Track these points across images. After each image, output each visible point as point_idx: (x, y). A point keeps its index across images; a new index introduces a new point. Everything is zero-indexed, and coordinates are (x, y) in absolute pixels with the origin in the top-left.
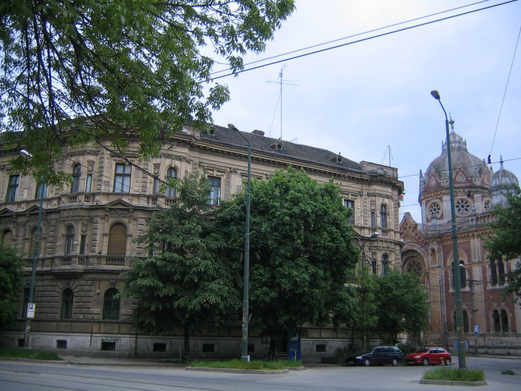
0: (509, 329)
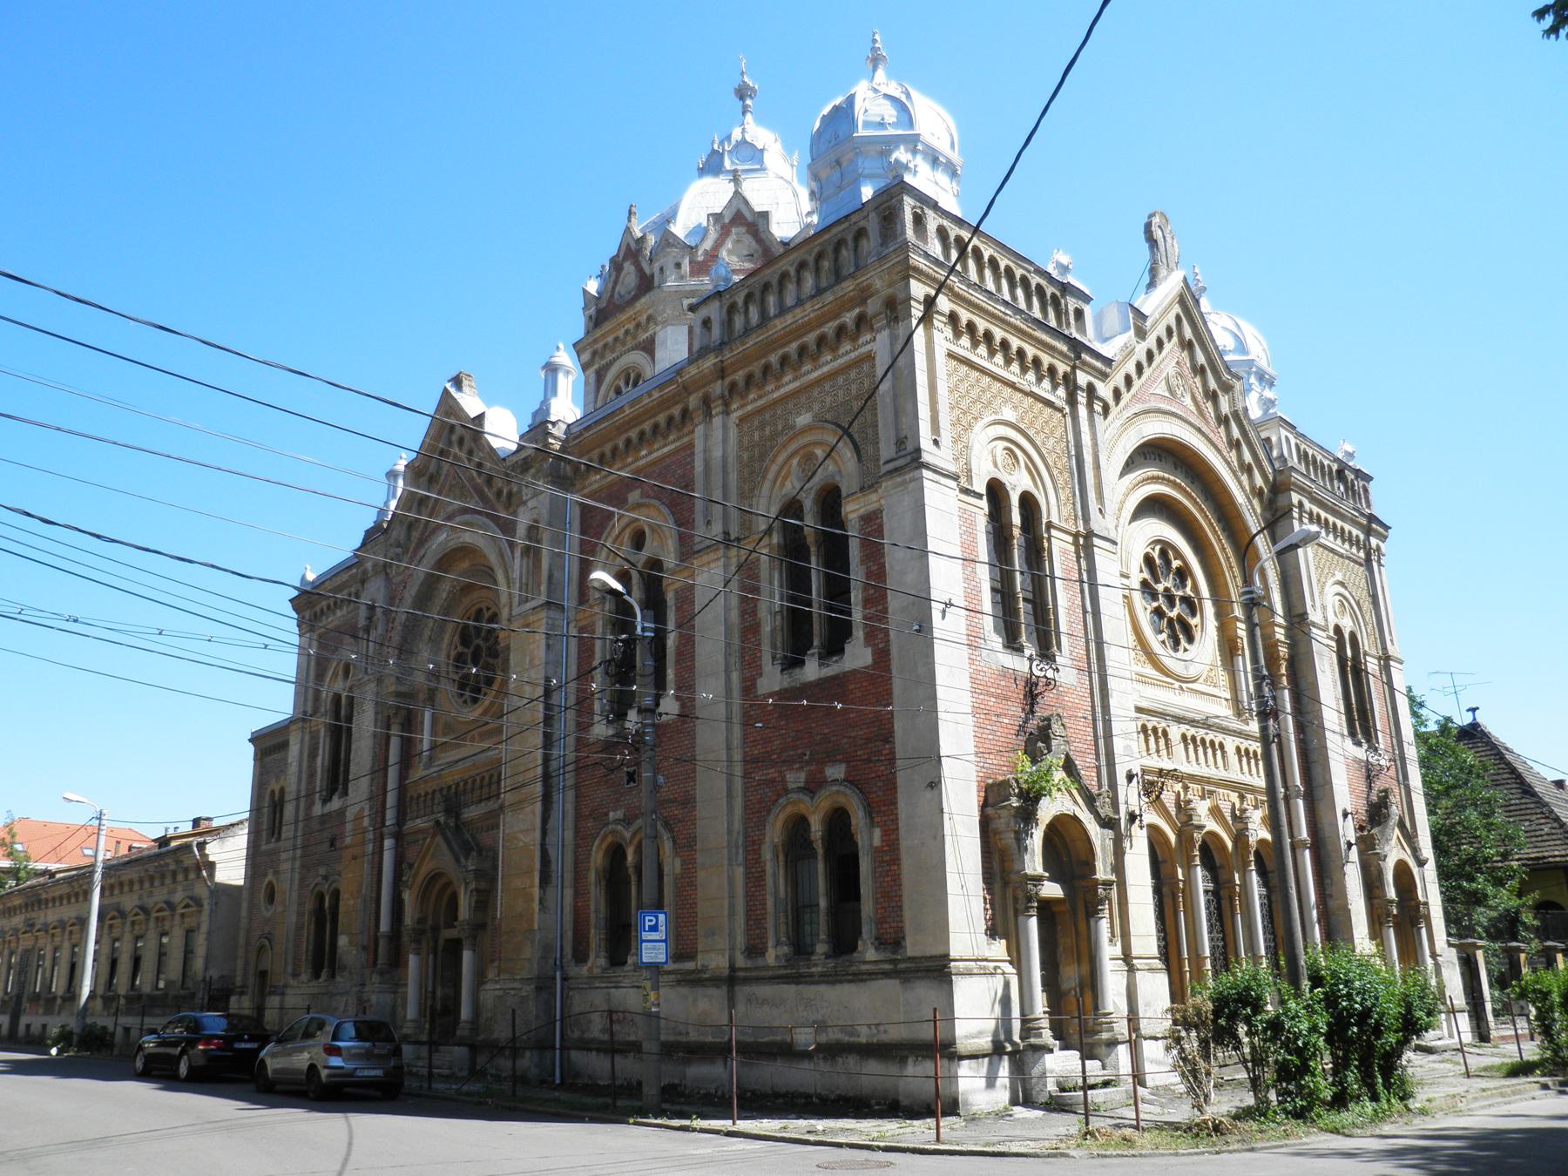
0: (867, 931)
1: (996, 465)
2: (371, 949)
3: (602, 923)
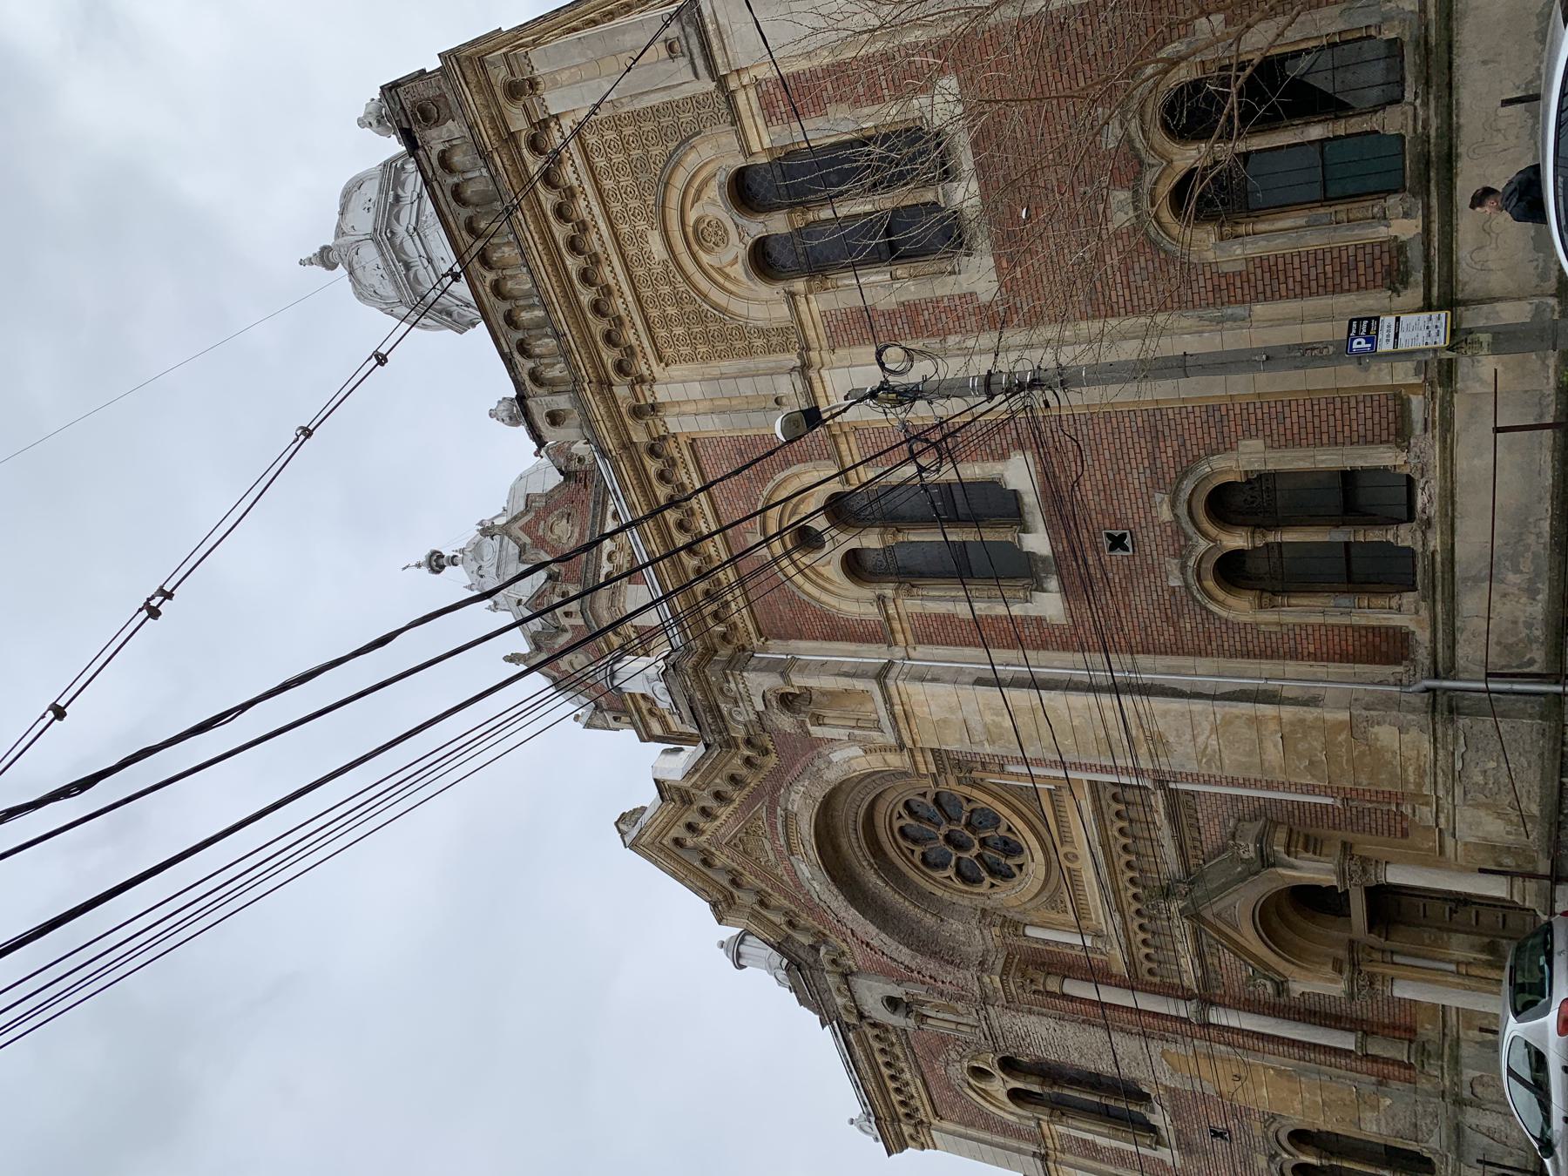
2: (1384, 1072)
3: (1344, 601)
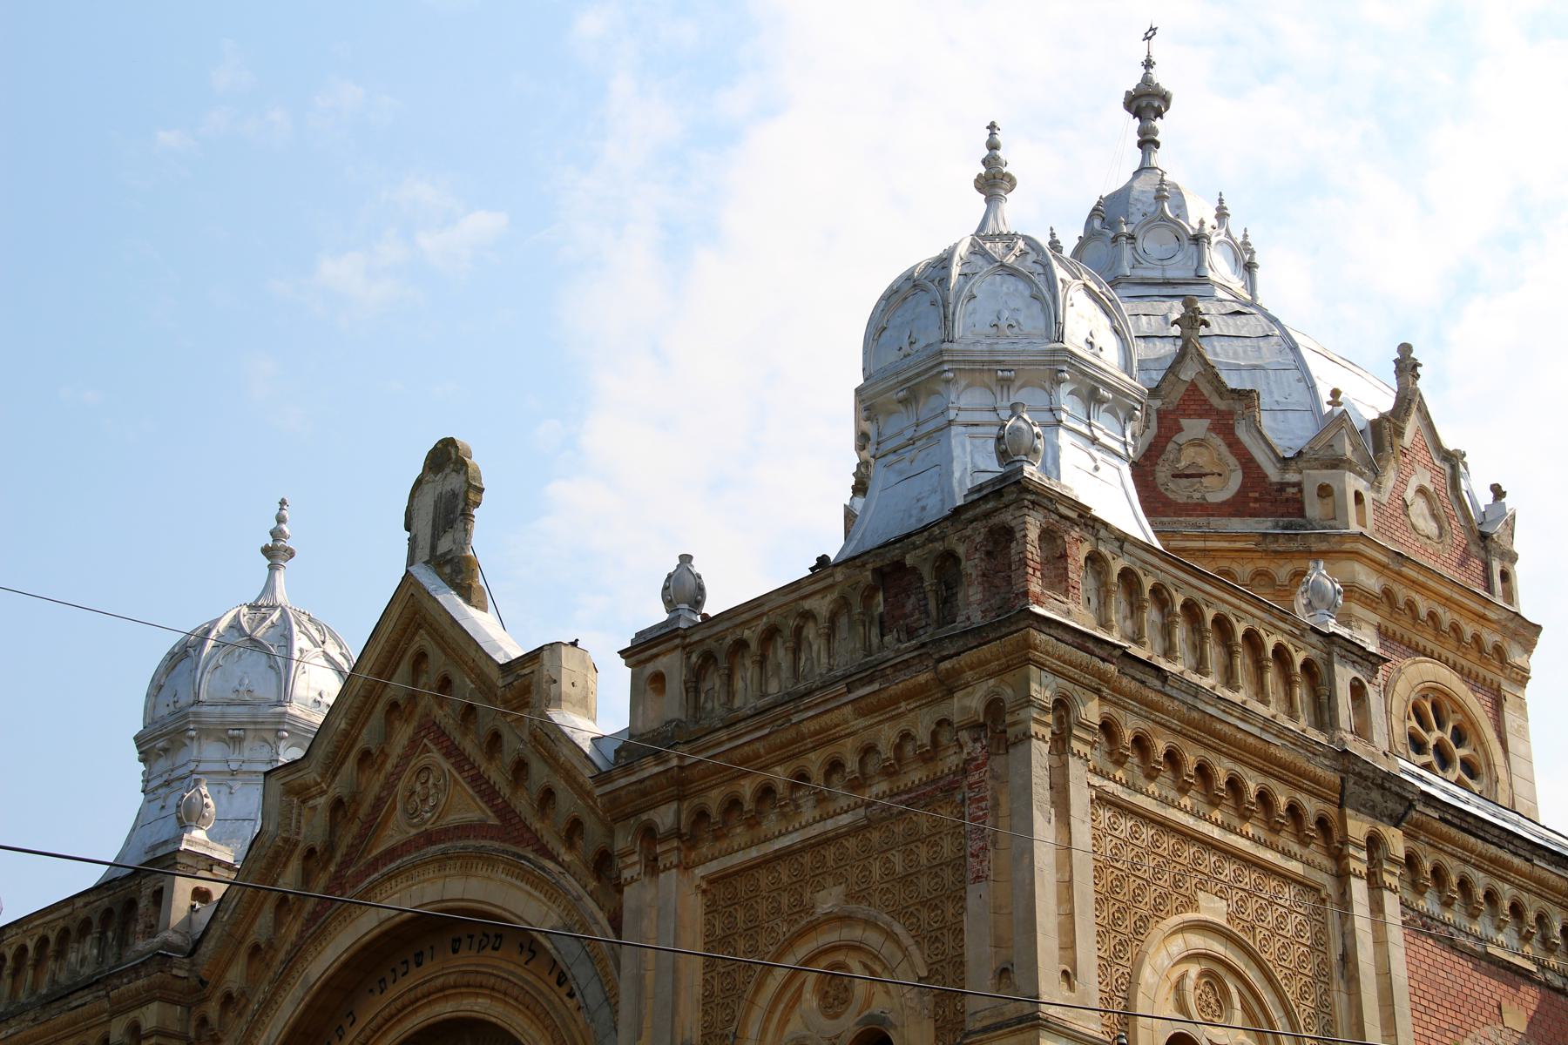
1: (1182, 1006)
